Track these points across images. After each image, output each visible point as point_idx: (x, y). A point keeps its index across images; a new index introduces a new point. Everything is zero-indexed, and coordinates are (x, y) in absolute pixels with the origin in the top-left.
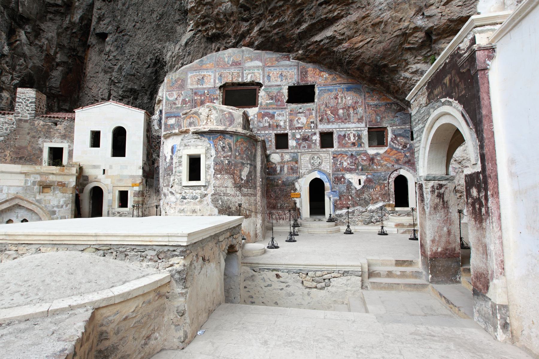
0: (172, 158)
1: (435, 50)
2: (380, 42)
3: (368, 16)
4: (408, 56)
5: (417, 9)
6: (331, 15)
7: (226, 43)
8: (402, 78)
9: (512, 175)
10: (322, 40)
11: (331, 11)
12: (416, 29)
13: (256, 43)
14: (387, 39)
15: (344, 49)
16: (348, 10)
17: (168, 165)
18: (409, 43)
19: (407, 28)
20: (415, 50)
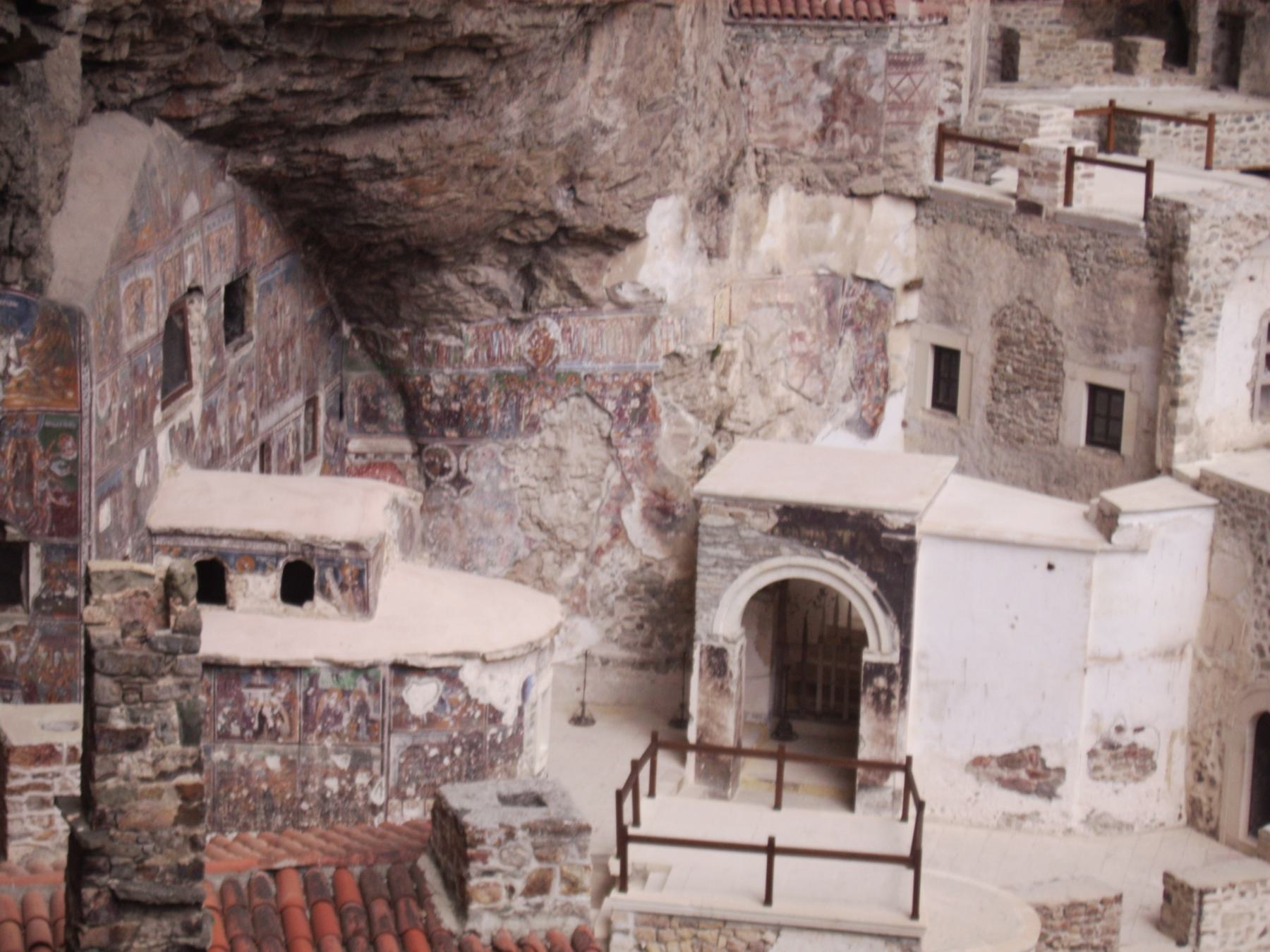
0: (521, 711)
1: (547, 259)
2: (470, 209)
3: (480, 143)
4: (487, 251)
5: (566, 173)
6: (415, 109)
7: (113, 88)
8: (436, 283)
9: (920, 667)
10: (356, 160)
11: (426, 101)
12: (552, 215)
13: (206, 122)
14: (484, 208)
15: (385, 198)
16: (450, 108)
17: (510, 732)
18: (518, 233)
19: (536, 205)
20: (507, 246)
